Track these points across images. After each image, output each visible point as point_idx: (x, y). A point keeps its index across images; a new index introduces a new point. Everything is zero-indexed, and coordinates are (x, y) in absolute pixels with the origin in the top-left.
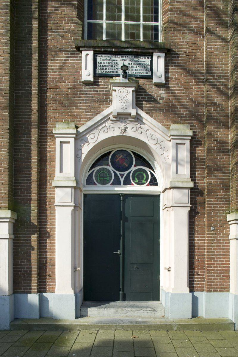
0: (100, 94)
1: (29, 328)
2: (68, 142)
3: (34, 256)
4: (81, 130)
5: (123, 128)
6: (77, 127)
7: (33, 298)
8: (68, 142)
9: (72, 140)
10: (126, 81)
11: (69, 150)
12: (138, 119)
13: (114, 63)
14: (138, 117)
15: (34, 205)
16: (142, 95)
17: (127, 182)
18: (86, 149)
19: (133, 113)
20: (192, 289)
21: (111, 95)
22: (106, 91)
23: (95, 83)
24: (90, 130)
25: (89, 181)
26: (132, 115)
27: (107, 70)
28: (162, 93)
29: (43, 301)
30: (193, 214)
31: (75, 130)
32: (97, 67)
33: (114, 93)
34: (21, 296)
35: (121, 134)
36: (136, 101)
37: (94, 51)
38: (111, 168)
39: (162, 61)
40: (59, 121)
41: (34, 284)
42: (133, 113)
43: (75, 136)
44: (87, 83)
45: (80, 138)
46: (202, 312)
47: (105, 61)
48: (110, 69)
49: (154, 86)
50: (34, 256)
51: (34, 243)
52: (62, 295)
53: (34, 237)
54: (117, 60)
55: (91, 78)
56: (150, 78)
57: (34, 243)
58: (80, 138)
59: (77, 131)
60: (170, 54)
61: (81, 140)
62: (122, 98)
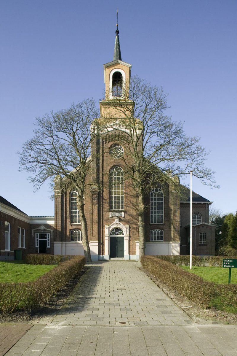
1: (101, 260)
3: (102, 248)
7: (102, 256)
9: (108, 228)
11: (108, 230)
12: (120, 224)
15: (101, 239)
17: (118, 234)
18: (110, 229)
19: (119, 223)
20: (129, 254)
23: (112, 217)
24: (111, 226)
25: (111, 234)
29: (103, 257)
30: (129, 241)
34: (99, 256)
38: (115, 232)
39: (124, 213)
41: (102, 253)
42: (119, 223)
45: (109, 228)
46: (131, 259)
50: (102, 248)
51: (102, 246)
52: (106, 255)
53: (102, 245)
56: (122, 216)
57: (102, 246)
58: (109, 228)
60: (125, 212)
62: (117, 220)
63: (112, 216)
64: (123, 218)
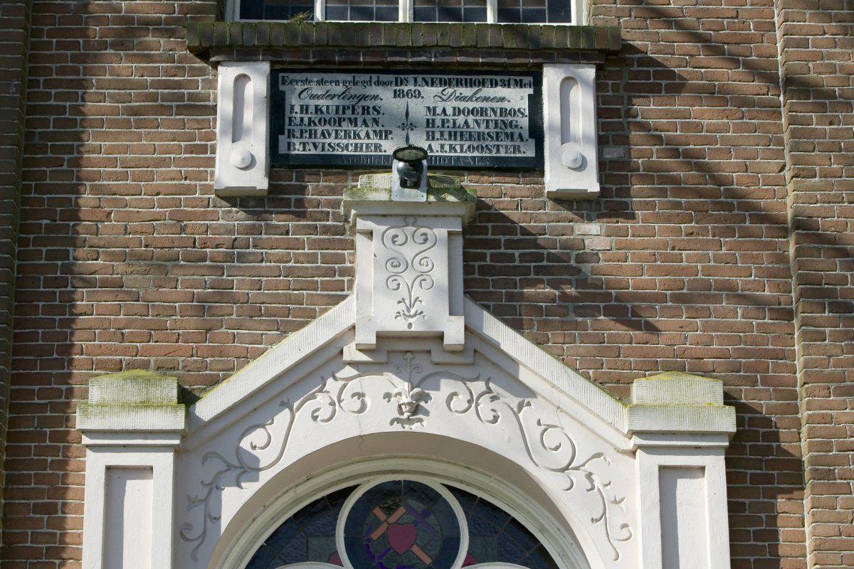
0: (299, 245)
2: (146, 471)
4: (210, 406)
5: (405, 399)
6: (187, 398)
8: (146, 471)
9: (163, 463)
10: (419, 196)
11: (150, 507)
12: (477, 358)
13: (365, 110)
14: (477, 345)
16: (495, 244)
19: (454, 332)
21: (352, 245)
22: (327, 230)
26: (448, 341)
27: (332, 140)
28: (593, 233)
31: (181, 414)
32: (287, 127)
33: (360, 240)
35: (397, 428)
36: (467, 270)
37: (273, 63)
40: (104, 366)
42: (454, 332)
43: (177, 442)
44: (238, 199)
47: (321, 102)
48: (347, 135)
49: (550, 204)
54: (376, 97)
55: (258, 180)
56: (534, 167)
58: (204, 455)
59: (189, 416)
61: (205, 458)
63: (277, 160)
64: (565, 200)
